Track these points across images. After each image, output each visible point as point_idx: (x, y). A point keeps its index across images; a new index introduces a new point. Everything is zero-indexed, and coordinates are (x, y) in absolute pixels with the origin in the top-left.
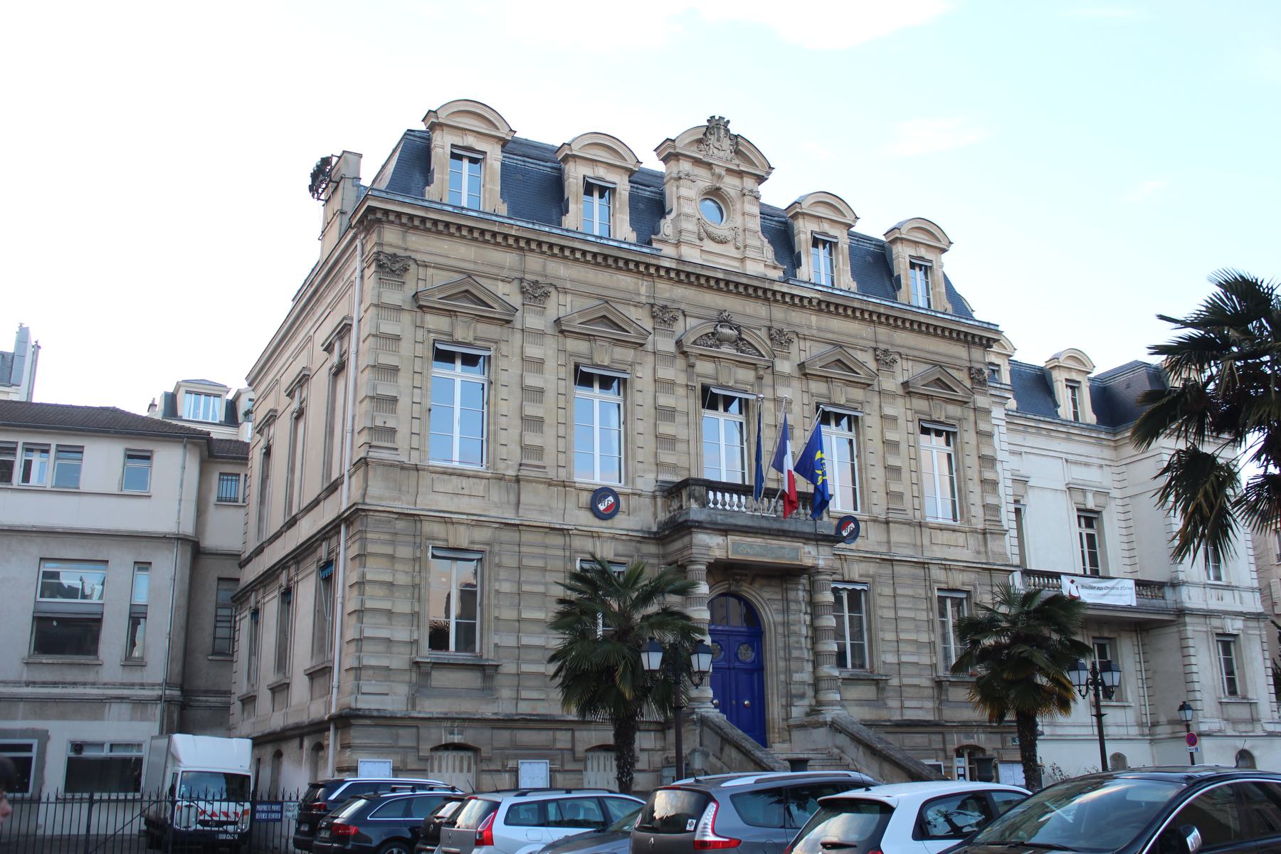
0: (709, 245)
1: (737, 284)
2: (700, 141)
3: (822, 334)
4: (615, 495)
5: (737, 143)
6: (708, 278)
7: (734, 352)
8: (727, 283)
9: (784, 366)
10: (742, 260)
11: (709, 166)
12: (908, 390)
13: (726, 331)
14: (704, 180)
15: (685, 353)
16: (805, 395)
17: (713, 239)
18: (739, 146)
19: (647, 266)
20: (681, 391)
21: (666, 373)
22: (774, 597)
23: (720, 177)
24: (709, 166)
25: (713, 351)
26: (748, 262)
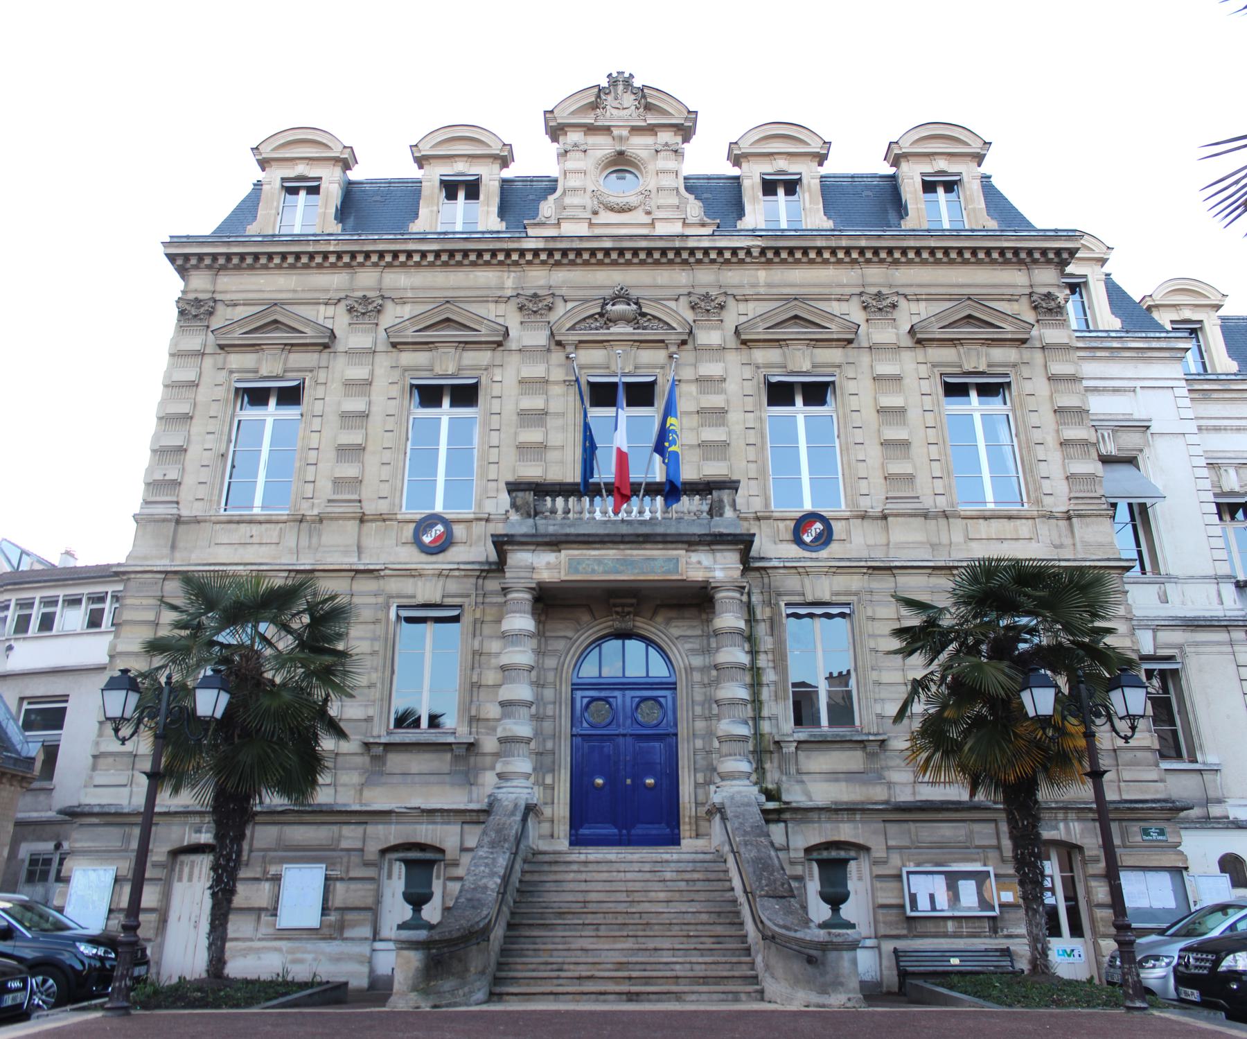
0: (606, 217)
1: (635, 252)
2: (594, 106)
3: (775, 291)
4: (447, 523)
5: (644, 97)
6: (593, 252)
7: (630, 330)
8: (621, 252)
9: (709, 337)
10: (652, 224)
11: (607, 130)
12: (920, 340)
13: (621, 307)
14: (603, 147)
15: (559, 343)
17: (612, 210)
18: (646, 99)
19: (508, 253)
20: (556, 390)
21: (536, 370)
22: (689, 633)
23: (621, 139)
24: (607, 130)
25: (602, 334)
26: (657, 224)
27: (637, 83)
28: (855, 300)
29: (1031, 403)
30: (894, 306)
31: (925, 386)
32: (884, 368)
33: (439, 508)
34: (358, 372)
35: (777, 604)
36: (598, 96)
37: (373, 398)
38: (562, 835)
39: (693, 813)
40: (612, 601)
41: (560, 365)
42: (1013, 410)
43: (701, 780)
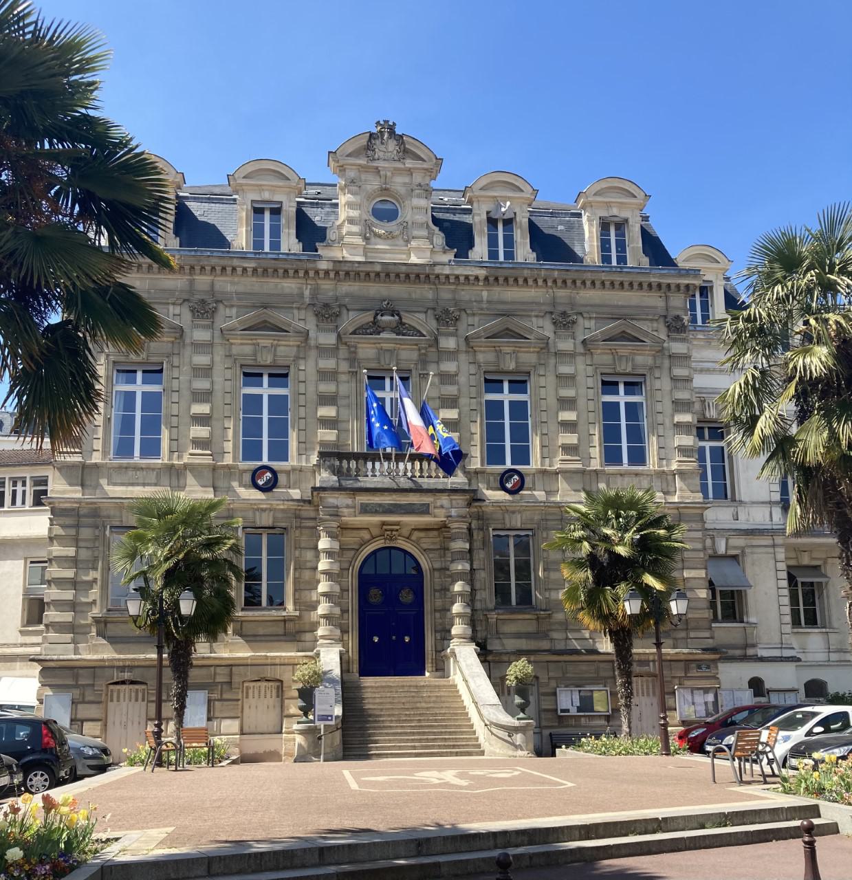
7: (394, 336)
9: (449, 343)
13: (387, 318)
16: (472, 366)
20: (343, 378)
27: (398, 131)
28: (548, 315)
29: (658, 395)
30: (574, 322)
31: (590, 382)
32: (565, 369)
33: (265, 461)
34: (202, 360)
35: (488, 529)
36: (370, 140)
37: (215, 379)
38: (355, 670)
39: (434, 657)
40: (385, 527)
41: (344, 359)
42: (647, 400)
43: (439, 638)
